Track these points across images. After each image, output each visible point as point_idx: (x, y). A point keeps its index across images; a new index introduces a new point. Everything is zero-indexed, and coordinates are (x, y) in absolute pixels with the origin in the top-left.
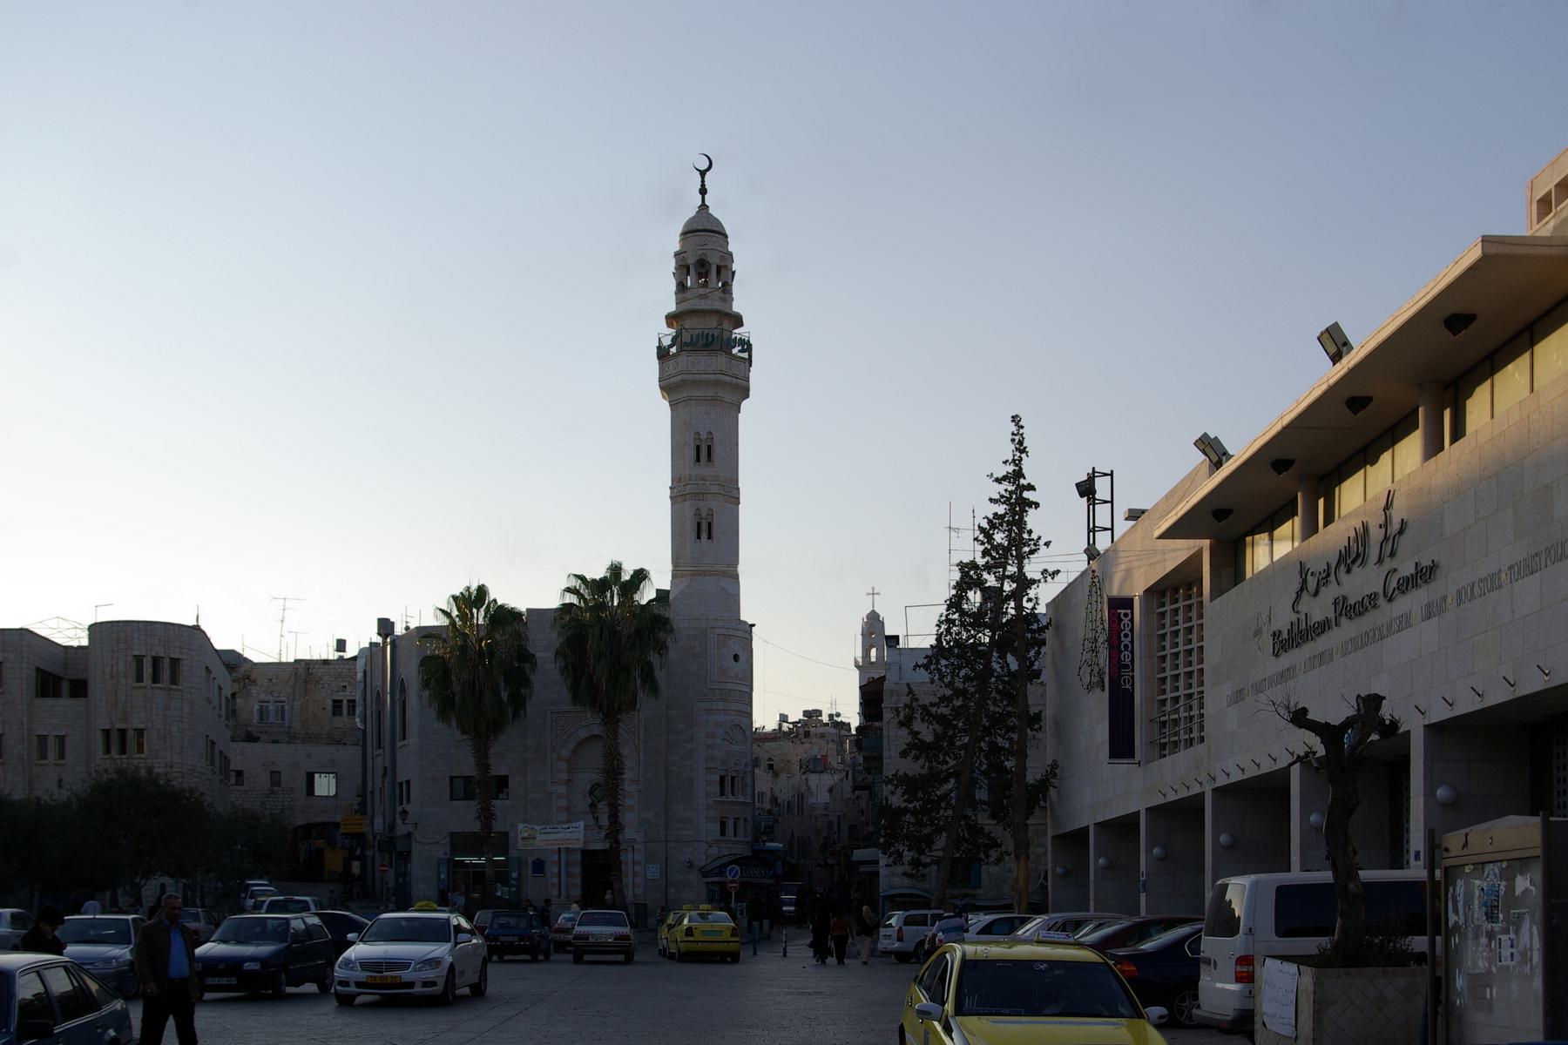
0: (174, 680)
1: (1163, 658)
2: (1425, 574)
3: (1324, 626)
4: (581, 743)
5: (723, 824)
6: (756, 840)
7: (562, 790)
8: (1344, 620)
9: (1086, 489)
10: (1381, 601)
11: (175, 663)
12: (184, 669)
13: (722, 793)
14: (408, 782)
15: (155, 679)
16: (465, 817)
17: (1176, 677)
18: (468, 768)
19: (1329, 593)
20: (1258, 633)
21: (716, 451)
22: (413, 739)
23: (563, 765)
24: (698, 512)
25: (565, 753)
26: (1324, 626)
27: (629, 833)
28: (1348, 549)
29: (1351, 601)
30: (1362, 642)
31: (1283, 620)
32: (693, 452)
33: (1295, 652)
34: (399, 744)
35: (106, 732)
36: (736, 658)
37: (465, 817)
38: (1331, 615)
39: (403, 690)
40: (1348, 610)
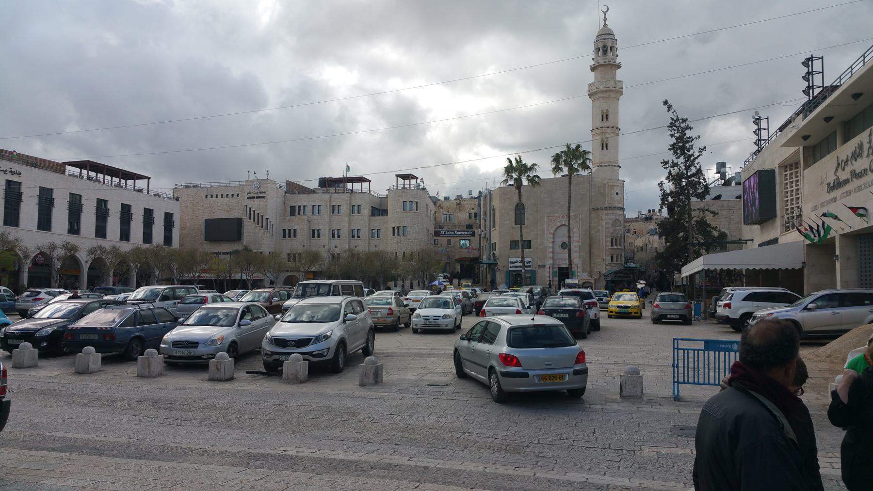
1: (787, 192)
3: (847, 181)
4: (558, 228)
5: (612, 257)
6: (626, 263)
7: (551, 245)
8: (854, 180)
10: (869, 172)
13: (612, 245)
17: (792, 200)
18: (517, 238)
19: (848, 169)
20: (822, 183)
21: (610, 116)
22: (497, 228)
23: (551, 236)
24: (602, 140)
25: (552, 231)
26: (847, 181)
28: (855, 151)
29: (857, 172)
31: (831, 179)
32: (600, 117)
33: (836, 191)
35: (394, 228)
38: (850, 177)
40: (856, 175)
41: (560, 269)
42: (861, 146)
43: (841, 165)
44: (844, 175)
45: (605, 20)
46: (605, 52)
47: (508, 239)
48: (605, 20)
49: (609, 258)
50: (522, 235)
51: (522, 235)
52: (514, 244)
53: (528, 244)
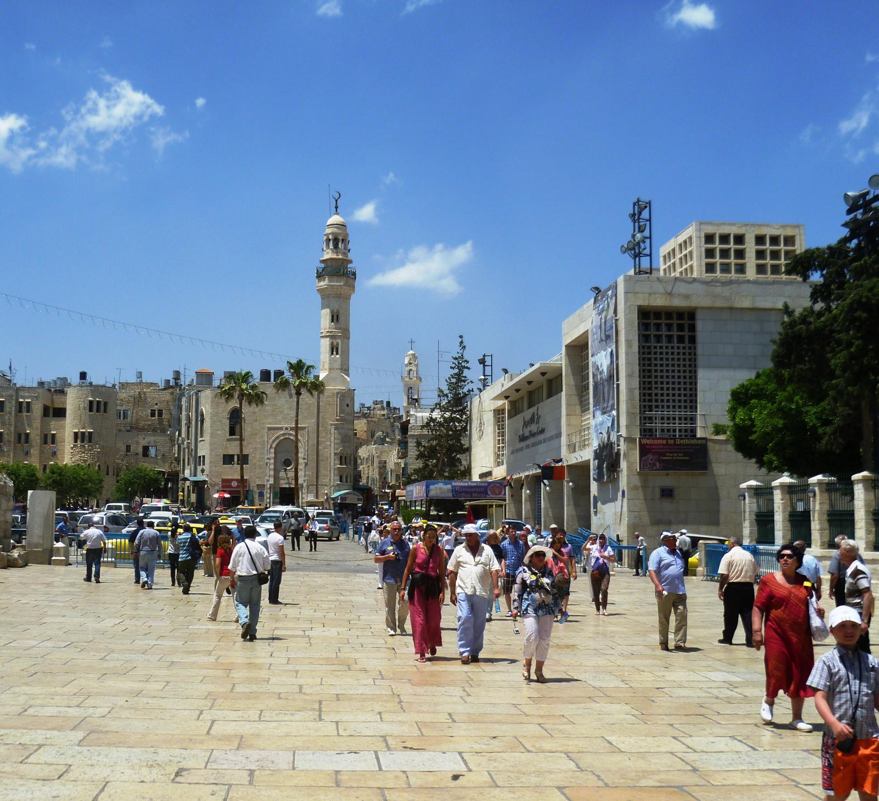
0: (105, 411)
2: (542, 431)
9: (482, 362)
11: (106, 404)
12: (109, 407)
14: (204, 457)
15: (98, 411)
16: (232, 472)
22: (207, 437)
24: (332, 344)
27: (300, 481)
30: (534, 445)
31: (521, 433)
34: (200, 439)
36: (348, 405)
37: (232, 472)
39: (202, 415)
41: (282, 489)
42: (533, 415)
43: (526, 424)
44: (527, 434)
45: (336, 207)
46: (336, 246)
47: (222, 452)
48: (336, 207)
49: (338, 478)
50: (241, 450)
51: (241, 450)
52: (228, 459)
53: (244, 459)
